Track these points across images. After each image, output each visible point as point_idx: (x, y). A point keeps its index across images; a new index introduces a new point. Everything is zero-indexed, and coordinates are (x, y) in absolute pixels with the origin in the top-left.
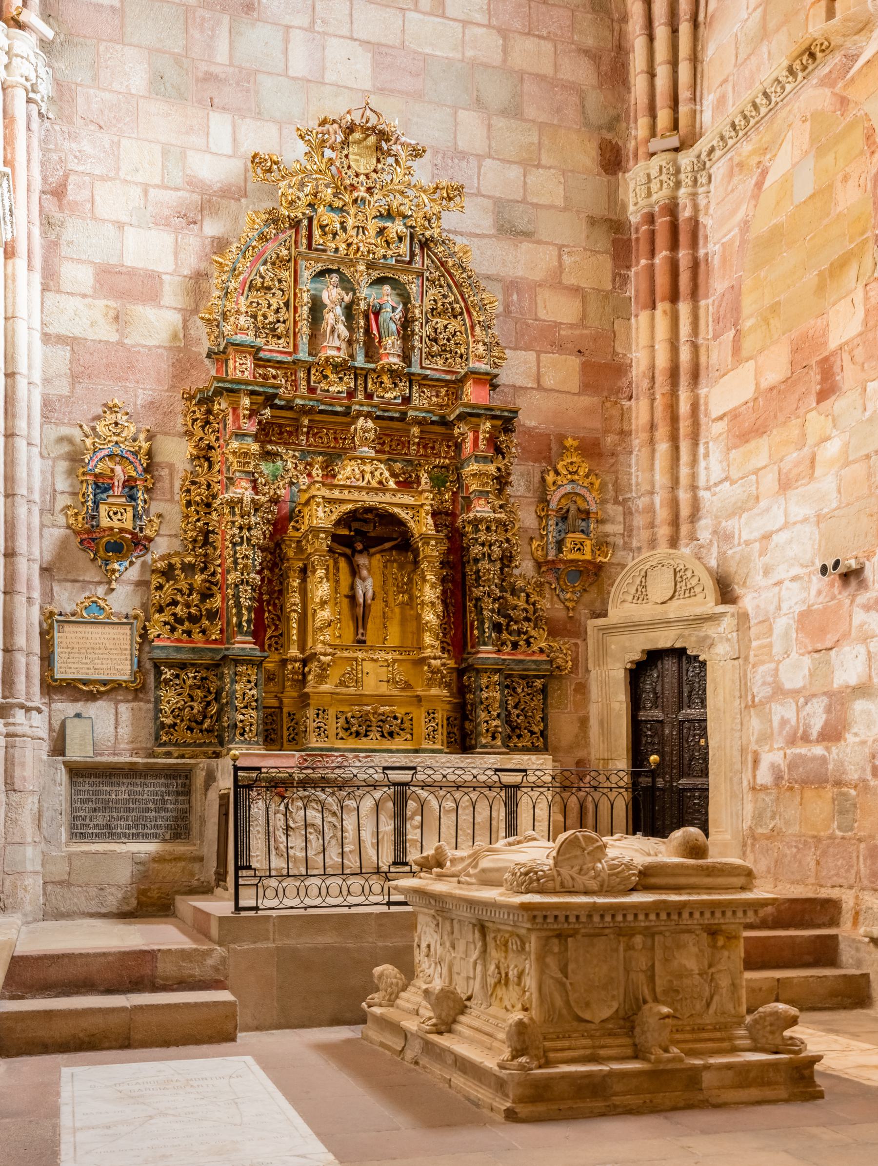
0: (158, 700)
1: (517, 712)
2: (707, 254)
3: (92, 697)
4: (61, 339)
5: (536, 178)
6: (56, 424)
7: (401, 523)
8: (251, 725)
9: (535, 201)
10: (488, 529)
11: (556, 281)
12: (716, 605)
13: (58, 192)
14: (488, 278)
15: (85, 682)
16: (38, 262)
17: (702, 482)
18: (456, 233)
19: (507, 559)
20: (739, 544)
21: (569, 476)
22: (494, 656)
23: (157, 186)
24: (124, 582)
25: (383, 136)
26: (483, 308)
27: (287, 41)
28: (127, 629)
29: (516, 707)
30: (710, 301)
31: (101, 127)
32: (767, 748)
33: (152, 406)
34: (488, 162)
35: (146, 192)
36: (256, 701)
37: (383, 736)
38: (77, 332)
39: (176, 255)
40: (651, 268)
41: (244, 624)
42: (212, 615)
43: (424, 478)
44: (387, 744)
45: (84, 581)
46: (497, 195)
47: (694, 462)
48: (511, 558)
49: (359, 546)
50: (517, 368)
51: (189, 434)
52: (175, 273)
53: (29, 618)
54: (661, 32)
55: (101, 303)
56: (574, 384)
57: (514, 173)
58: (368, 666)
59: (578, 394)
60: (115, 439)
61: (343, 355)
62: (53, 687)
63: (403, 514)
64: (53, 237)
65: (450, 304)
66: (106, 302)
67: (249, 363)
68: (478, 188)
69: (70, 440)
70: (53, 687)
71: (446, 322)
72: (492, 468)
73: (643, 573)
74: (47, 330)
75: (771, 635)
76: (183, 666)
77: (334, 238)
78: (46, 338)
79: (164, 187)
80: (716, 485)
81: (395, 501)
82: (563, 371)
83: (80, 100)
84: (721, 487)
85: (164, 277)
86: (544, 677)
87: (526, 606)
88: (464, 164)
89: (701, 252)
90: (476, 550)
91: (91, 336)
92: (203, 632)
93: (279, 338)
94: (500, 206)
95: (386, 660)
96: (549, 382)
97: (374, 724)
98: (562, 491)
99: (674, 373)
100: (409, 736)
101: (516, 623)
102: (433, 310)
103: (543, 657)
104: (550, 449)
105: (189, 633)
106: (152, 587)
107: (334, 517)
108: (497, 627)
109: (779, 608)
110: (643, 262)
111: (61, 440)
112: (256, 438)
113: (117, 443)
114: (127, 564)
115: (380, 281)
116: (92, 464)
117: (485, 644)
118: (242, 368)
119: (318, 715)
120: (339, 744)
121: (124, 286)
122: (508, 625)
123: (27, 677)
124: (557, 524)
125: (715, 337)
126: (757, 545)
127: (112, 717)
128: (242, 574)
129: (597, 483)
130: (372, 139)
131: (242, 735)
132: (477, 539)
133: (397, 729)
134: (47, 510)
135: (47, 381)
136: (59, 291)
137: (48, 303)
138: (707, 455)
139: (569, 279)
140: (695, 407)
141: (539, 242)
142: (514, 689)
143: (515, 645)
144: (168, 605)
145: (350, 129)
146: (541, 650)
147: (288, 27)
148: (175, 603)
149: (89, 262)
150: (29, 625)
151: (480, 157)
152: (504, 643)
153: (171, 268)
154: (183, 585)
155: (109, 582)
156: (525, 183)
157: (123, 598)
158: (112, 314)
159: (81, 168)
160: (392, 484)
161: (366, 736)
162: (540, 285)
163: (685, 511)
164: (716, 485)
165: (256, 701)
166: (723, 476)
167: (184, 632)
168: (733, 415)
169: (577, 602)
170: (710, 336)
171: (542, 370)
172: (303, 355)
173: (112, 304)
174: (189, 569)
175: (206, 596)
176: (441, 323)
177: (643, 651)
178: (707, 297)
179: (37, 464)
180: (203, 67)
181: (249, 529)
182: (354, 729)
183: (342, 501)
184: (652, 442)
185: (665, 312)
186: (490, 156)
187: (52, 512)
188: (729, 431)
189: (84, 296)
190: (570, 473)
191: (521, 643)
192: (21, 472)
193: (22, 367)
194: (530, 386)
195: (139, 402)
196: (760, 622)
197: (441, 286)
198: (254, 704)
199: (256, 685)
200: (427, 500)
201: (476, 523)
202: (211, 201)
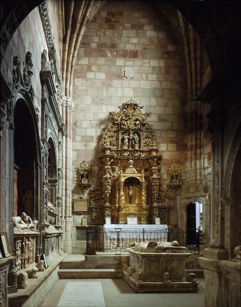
0: (92, 215)
4: (76, 150)
7: (138, 179)
13: (75, 124)
16: (72, 137)
19: (160, 185)
25: (136, 105)
26: (155, 137)
27: (117, 90)
38: (78, 148)
42: (102, 199)
43: (143, 171)
48: (161, 185)
51: (98, 165)
52: (96, 136)
53: (70, 200)
54: (194, 77)
56: (175, 149)
57: (163, 108)
58: (131, 208)
61: (127, 148)
62: (74, 213)
63: (138, 178)
67: (109, 151)
69: (77, 168)
70: (74, 213)
72: (157, 168)
76: (97, 208)
78: (73, 150)
79: (94, 120)
81: (137, 175)
83: (79, 107)
92: (101, 202)
105: (98, 202)
108: (158, 199)
112: (110, 165)
115: (134, 133)
118: (108, 152)
121: (86, 139)
123: (69, 211)
130: (133, 106)
134: (73, 181)
139: (174, 128)
143: (162, 202)
145: (128, 105)
147: (117, 87)
148: (95, 197)
150: (69, 202)
157: (85, 196)
160: (136, 172)
172: (119, 149)
174: (98, 190)
175: (101, 195)
176: (147, 140)
179: (71, 173)
180: (101, 97)
192: (68, 175)
193: (68, 156)
200: (143, 175)
201: (153, 179)
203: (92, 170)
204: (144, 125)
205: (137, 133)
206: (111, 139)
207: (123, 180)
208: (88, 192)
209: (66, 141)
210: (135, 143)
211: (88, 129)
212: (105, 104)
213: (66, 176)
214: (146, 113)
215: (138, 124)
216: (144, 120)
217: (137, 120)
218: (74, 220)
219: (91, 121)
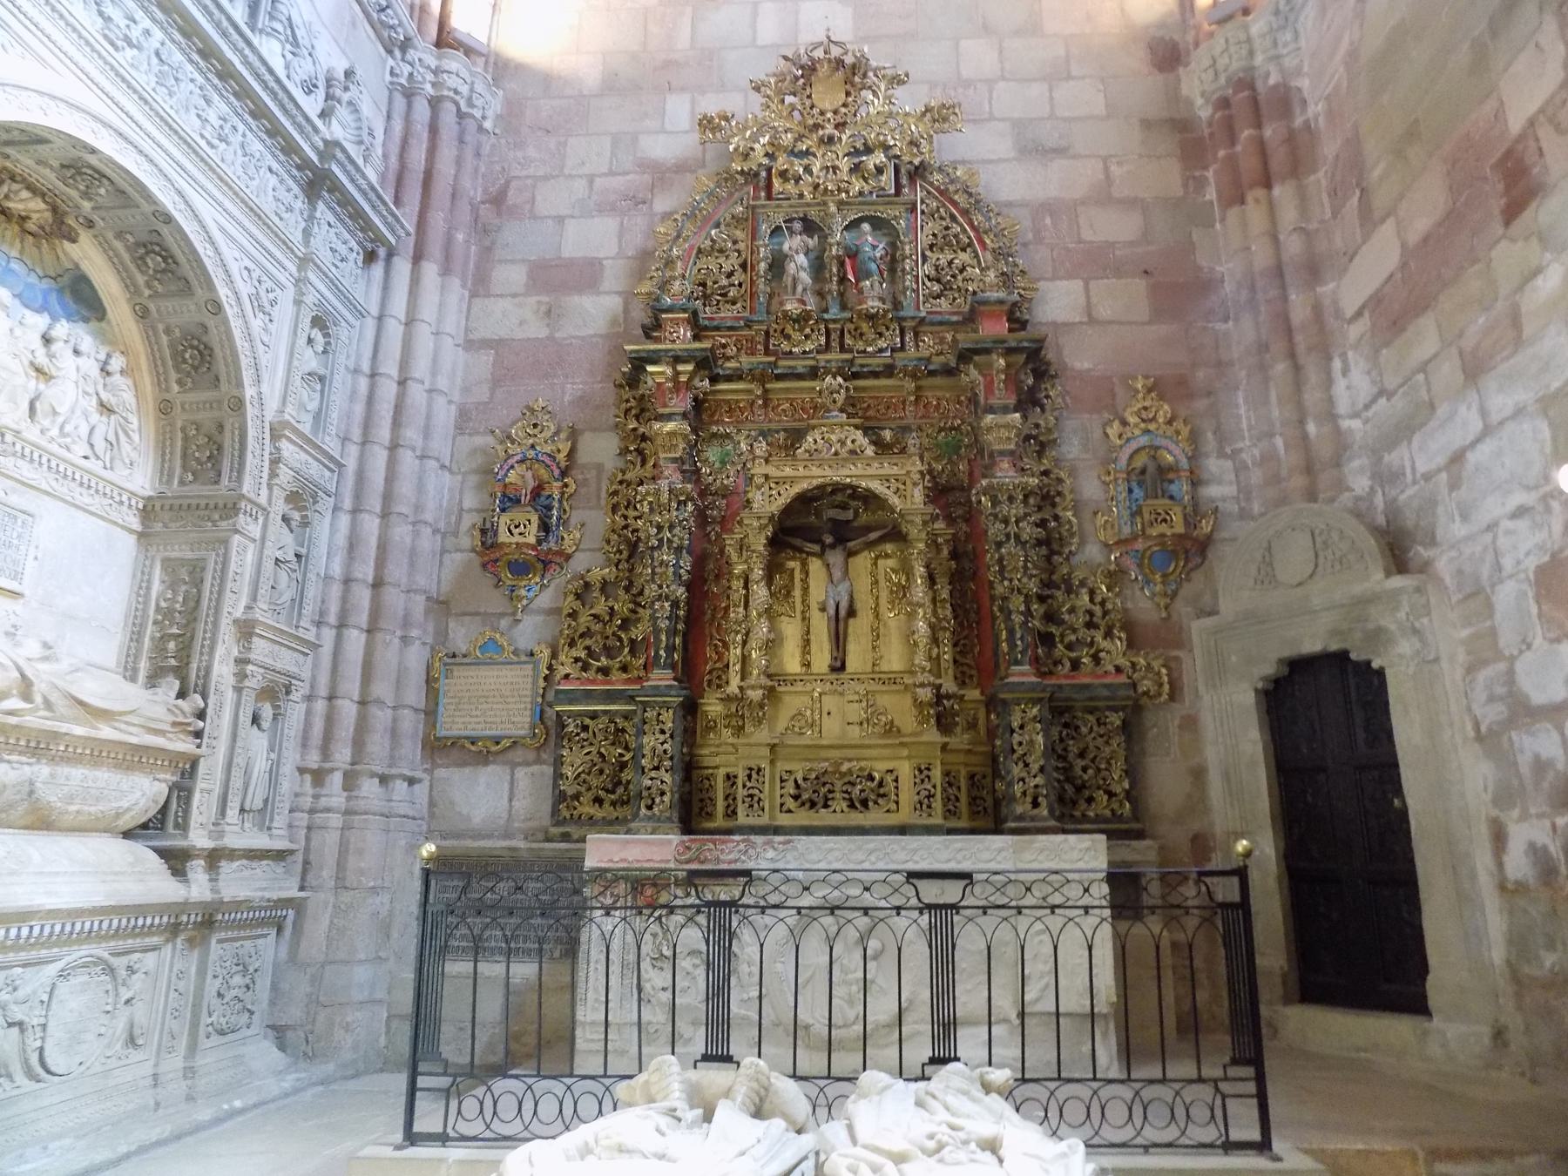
1: (1080, 763)
2: (1307, 122)
3: (484, 758)
4: (486, 344)
8: (663, 794)
9: (1067, 114)
10: (1011, 499)
11: (1103, 196)
12: (1388, 574)
13: (498, 200)
17: (1342, 407)
19: (1051, 544)
20: (1415, 482)
21: (1143, 425)
24: (533, 612)
29: (1082, 755)
30: (1321, 174)
32: (1516, 813)
33: (582, 401)
34: (1001, 84)
35: (591, 181)
36: (671, 758)
37: (852, 806)
38: (503, 333)
39: (620, 236)
40: (1232, 161)
41: (662, 652)
44: (857, 818)
45: (486, 614)
46: (1016, 115)
47: (1328, 382)
49: (829, 540)
50: (1057, 303)
55: (533, 300)
56: (1143, 311)
59: (1150, 323)
63: (876, 486)
64: (487, 243)
65: (955, 236)
68: (991, 113)
70: (439, 748)
71: (950, 257)
73: (1265, 545)
74: (471, 336)
75: (1491, 615)
77: (797, 182)
79: (611, 173)
80: (1367, 407)
81: (870, 474)
82: (1122, 299)
84: (1374, 408)
86: (1123, 708)
87: (1089, 606)
89: (1298, 122)
90: (995, 530)
91: (519, 334)
93: (734, 303)
94: (1019, 125)
96: (1104, 312)
97: (838, 787)
98: (1134, 445)
99: (1278, 271)
100: (894, 807)
101: (1074, 631)
102: (931, 247)
103: (1123, 679)
104: (1114, 396)
105: (605, 671)
106: (565, 612)
107: (781, 502)
109: (1498, 567)
110: (1221, 153)
111: (474, 451)
113: (533, 446)
116: (502, 473)
117: (1017, 663)
119: (749, 777)
120: (784, 820)
121: (558, 278)
122: (1062, 636)
124: (1130, 491)
125: (1335, 214)
126: (1444, 475)
127: (506, 786)
128: (660, 587)
129: (1185, 431)
131: (650, 808)
132: (996, 516)
133: (873, 797)
135: (466, 390)
136: (488, 296)
137: (475, 309)
138: (1345, 372)
140: (1317, 310)
142: (1077, 728)
143: (1076, 665)
144: (582, 636)
146: (1118, 670)
149: (523, 261)
151: (990, 83)
152: (1057, 663)
153: (614, 251)
155: (514, 614)
156: (1051, 98)
158: (543, 308)
159: (524, 173)
161: (826, 806)
162: (1083, 203)
163: (1324, 451)
164: (1367, 407)
165: (671, 758)
166: (1375, 390)
167: (599, 670)
168: (1376, 302)
170: (1328, 215)
171: (1094, 300)
173: (545, 299)
177: (1280, 661)
178: (1315, 171)
181: (671, 528)
182: (805, 796)
183: (792, 480)
184: (1263, 368)
185: (1257, 201)
186: (1003, 78)
187: (456, 534)
188: (1374, 325)
189: (514, 296)
190: (1143, 421)
196: (1468, 597)
197: (942, 218)
198: (667, 763)
199: (672, 736)
202: (661, 175)
203: (583, 457)
204: (919, 172)
205: (878, 224)
207: (767, 503)
209: (415, 281)
210: (863, 274)
211: (571, 227)
212: (683, 89)
213: (388, 497)
214: (928, 110)
215: (879, 170)
216: (914, 143)
217: (868, 150)
218: (432, 804)
219: (591, 179)
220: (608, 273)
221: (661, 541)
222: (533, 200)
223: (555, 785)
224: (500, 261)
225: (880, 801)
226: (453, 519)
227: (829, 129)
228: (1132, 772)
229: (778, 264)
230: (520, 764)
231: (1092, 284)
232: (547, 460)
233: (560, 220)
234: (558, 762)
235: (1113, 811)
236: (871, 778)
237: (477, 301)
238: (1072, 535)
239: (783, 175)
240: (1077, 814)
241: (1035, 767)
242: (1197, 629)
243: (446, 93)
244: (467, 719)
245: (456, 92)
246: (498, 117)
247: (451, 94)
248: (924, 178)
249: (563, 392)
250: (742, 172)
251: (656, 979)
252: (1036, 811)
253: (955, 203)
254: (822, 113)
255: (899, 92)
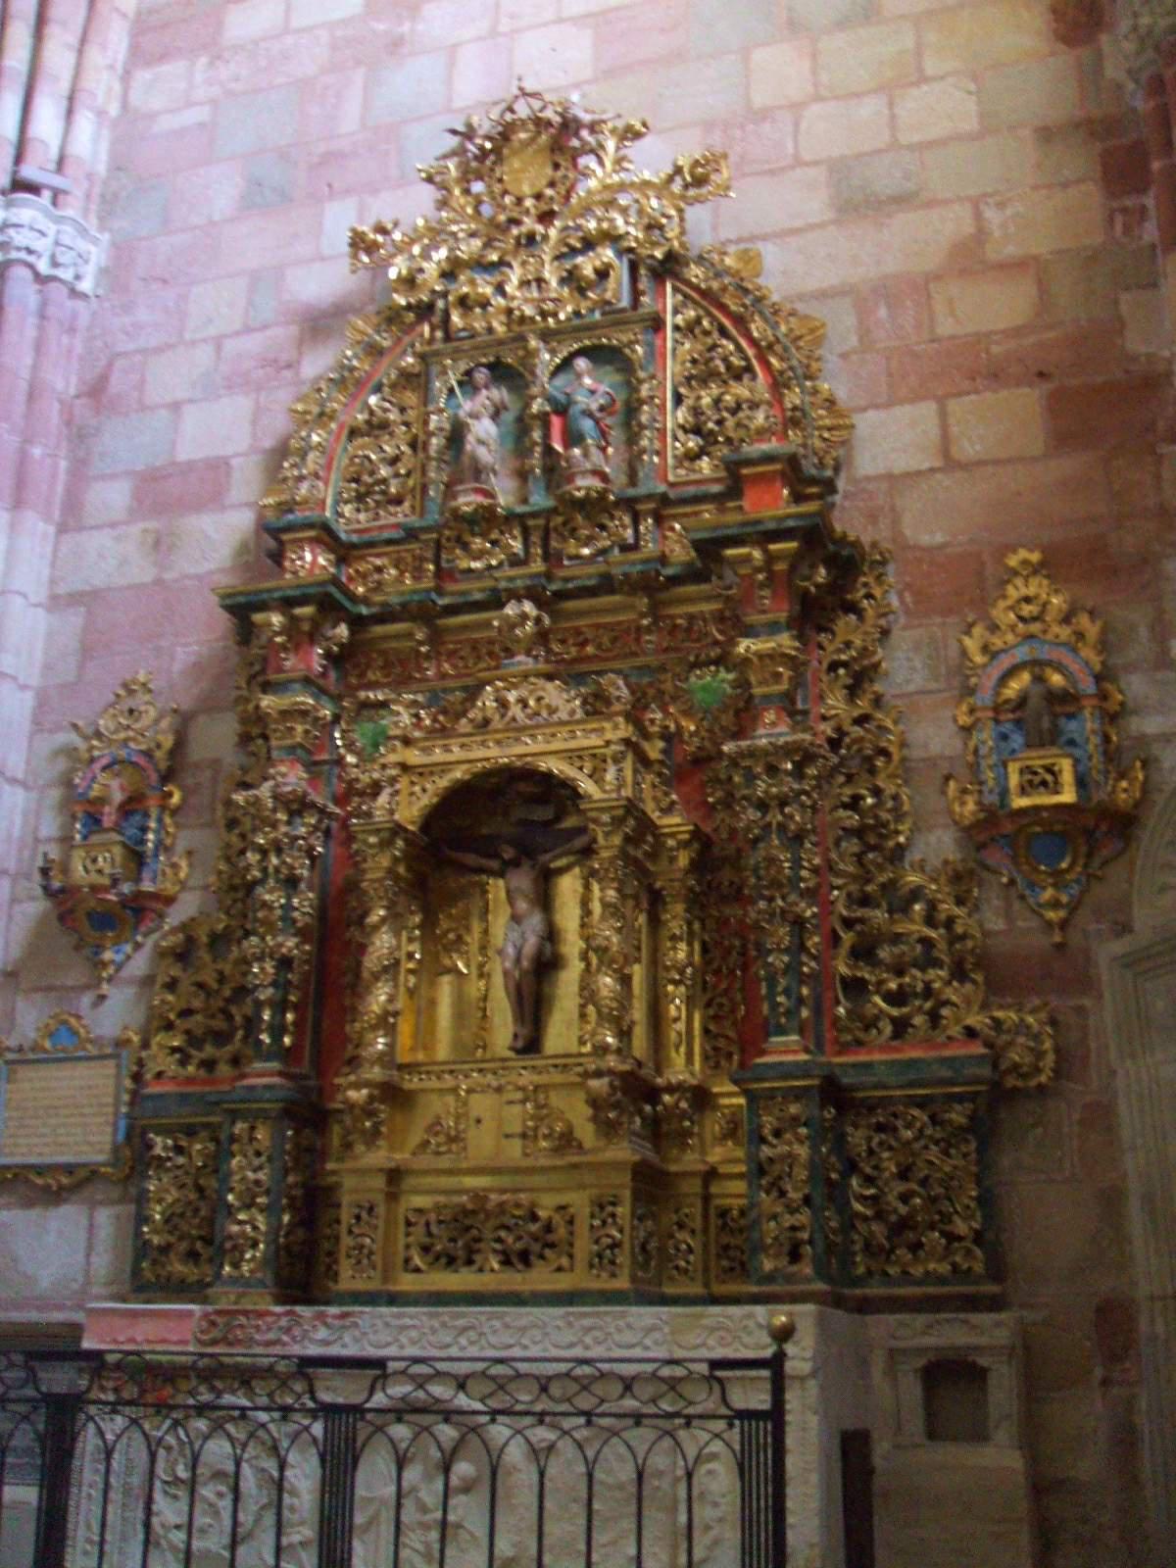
1: (901, 1187)
3: (55, 1196)
4: (75, 599)
5: (913, 104)
6: (51, 731)
9: (916, 138)
11: (969, 258)
14: (823, 295)
15: (40, 1170)
18: (753, 238)
22: (803, 1057)
23: (237, 334)
28: (109, 1068)
29: (904, 1174)
31: (165, 281)
34: (816, 108)
35: (219, 348)
37: (507, 1262)
38: (99, 581)
39: (254, 422)
46: (836, 153)
49: (508, 853)
50: (888, 441)
55: (135, 529)
56: (1035, 442)
60: (122, 735)
63: (556, 766)
66: (142, 525)
78: (58, 602)
79: (248, 330)
82: (1001, 422)
85: (234, 462)
86: (973, 1097)
88: (767, 127)
94: (839, 169)
95: (523, 1089)
97: (488, 1234)
98: (1006, 662)
100: (565, 1261)
103: (978, 1049)
105: (209, 1065)
111: (58, 752)
114: (128, 948)
119: (358, 1218)
120: (407, 1283)
121: (168, 493)
127: (83, 1235)
129: (1092, 630)
136: (80, 529)
137: (64, 549)
141: (930, 204)
143: (901, 1027)
146: (971, 1033)
151: (796, 107)
152: (870, 1024)
154: (209, 977)
156: (893, 117)
158: (150, 540)
159: (131, 347)
161: (470, 1262)
162: (938, 278)
165: (267, 1192)
169: (1073, 908)
171: (955, 430)
180: (322, 148)
183: (445, 767)
186: (818, 98)
189: (113, 525)
191: (918, 1020)
194: (926, 466)
195: (177, 667)
199: (270, 1159)
202: (318, 324)
203: (197, 752)
204: (669, 267)
206: (365, 448)
207: (408, 804)
208: (139, 964)
212: (348, 192)
215: (603, 274)
217: (589, 244)
219: (218, 342)
220: (236, 475)
221: (264, 870)
222: (142, 384)
223: (138, 1234)
224: (103, 478)
225: (548, 1252)
226: (26, 853)
227: (529, 224)
228: (985, 1201)
229: (456, 435)
230: (101, 1203)
231: (953, 405)
232: (142, 761)
233: (176, 407)
234: (142, 1199)
235: (954, 1265)
236: (534, 1218)
237: (66, 538)
238: (900, 817)
239: (463, 302)
240: (893, 1271)
241: (795, 1195)
242: (1108, 951)
243: (14, 255)
244: (36, 1140)
245: (30, 251)
246: (103, 272)
247: (23, 255)
248: (677, 276)
249: (173, 658)
250: (409, 307)
251: (169, 1511)
252: (794, 1268)
253: (723, 308)
254: (519, 201)
255: (633, 149)
